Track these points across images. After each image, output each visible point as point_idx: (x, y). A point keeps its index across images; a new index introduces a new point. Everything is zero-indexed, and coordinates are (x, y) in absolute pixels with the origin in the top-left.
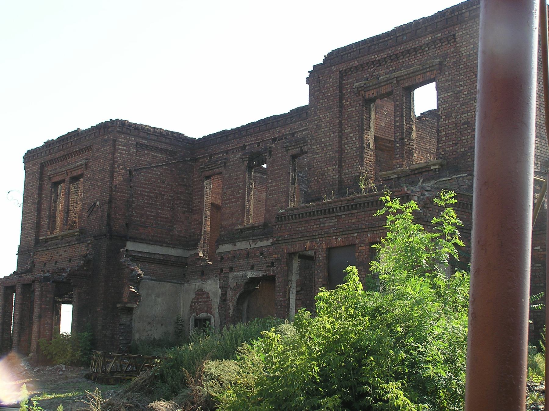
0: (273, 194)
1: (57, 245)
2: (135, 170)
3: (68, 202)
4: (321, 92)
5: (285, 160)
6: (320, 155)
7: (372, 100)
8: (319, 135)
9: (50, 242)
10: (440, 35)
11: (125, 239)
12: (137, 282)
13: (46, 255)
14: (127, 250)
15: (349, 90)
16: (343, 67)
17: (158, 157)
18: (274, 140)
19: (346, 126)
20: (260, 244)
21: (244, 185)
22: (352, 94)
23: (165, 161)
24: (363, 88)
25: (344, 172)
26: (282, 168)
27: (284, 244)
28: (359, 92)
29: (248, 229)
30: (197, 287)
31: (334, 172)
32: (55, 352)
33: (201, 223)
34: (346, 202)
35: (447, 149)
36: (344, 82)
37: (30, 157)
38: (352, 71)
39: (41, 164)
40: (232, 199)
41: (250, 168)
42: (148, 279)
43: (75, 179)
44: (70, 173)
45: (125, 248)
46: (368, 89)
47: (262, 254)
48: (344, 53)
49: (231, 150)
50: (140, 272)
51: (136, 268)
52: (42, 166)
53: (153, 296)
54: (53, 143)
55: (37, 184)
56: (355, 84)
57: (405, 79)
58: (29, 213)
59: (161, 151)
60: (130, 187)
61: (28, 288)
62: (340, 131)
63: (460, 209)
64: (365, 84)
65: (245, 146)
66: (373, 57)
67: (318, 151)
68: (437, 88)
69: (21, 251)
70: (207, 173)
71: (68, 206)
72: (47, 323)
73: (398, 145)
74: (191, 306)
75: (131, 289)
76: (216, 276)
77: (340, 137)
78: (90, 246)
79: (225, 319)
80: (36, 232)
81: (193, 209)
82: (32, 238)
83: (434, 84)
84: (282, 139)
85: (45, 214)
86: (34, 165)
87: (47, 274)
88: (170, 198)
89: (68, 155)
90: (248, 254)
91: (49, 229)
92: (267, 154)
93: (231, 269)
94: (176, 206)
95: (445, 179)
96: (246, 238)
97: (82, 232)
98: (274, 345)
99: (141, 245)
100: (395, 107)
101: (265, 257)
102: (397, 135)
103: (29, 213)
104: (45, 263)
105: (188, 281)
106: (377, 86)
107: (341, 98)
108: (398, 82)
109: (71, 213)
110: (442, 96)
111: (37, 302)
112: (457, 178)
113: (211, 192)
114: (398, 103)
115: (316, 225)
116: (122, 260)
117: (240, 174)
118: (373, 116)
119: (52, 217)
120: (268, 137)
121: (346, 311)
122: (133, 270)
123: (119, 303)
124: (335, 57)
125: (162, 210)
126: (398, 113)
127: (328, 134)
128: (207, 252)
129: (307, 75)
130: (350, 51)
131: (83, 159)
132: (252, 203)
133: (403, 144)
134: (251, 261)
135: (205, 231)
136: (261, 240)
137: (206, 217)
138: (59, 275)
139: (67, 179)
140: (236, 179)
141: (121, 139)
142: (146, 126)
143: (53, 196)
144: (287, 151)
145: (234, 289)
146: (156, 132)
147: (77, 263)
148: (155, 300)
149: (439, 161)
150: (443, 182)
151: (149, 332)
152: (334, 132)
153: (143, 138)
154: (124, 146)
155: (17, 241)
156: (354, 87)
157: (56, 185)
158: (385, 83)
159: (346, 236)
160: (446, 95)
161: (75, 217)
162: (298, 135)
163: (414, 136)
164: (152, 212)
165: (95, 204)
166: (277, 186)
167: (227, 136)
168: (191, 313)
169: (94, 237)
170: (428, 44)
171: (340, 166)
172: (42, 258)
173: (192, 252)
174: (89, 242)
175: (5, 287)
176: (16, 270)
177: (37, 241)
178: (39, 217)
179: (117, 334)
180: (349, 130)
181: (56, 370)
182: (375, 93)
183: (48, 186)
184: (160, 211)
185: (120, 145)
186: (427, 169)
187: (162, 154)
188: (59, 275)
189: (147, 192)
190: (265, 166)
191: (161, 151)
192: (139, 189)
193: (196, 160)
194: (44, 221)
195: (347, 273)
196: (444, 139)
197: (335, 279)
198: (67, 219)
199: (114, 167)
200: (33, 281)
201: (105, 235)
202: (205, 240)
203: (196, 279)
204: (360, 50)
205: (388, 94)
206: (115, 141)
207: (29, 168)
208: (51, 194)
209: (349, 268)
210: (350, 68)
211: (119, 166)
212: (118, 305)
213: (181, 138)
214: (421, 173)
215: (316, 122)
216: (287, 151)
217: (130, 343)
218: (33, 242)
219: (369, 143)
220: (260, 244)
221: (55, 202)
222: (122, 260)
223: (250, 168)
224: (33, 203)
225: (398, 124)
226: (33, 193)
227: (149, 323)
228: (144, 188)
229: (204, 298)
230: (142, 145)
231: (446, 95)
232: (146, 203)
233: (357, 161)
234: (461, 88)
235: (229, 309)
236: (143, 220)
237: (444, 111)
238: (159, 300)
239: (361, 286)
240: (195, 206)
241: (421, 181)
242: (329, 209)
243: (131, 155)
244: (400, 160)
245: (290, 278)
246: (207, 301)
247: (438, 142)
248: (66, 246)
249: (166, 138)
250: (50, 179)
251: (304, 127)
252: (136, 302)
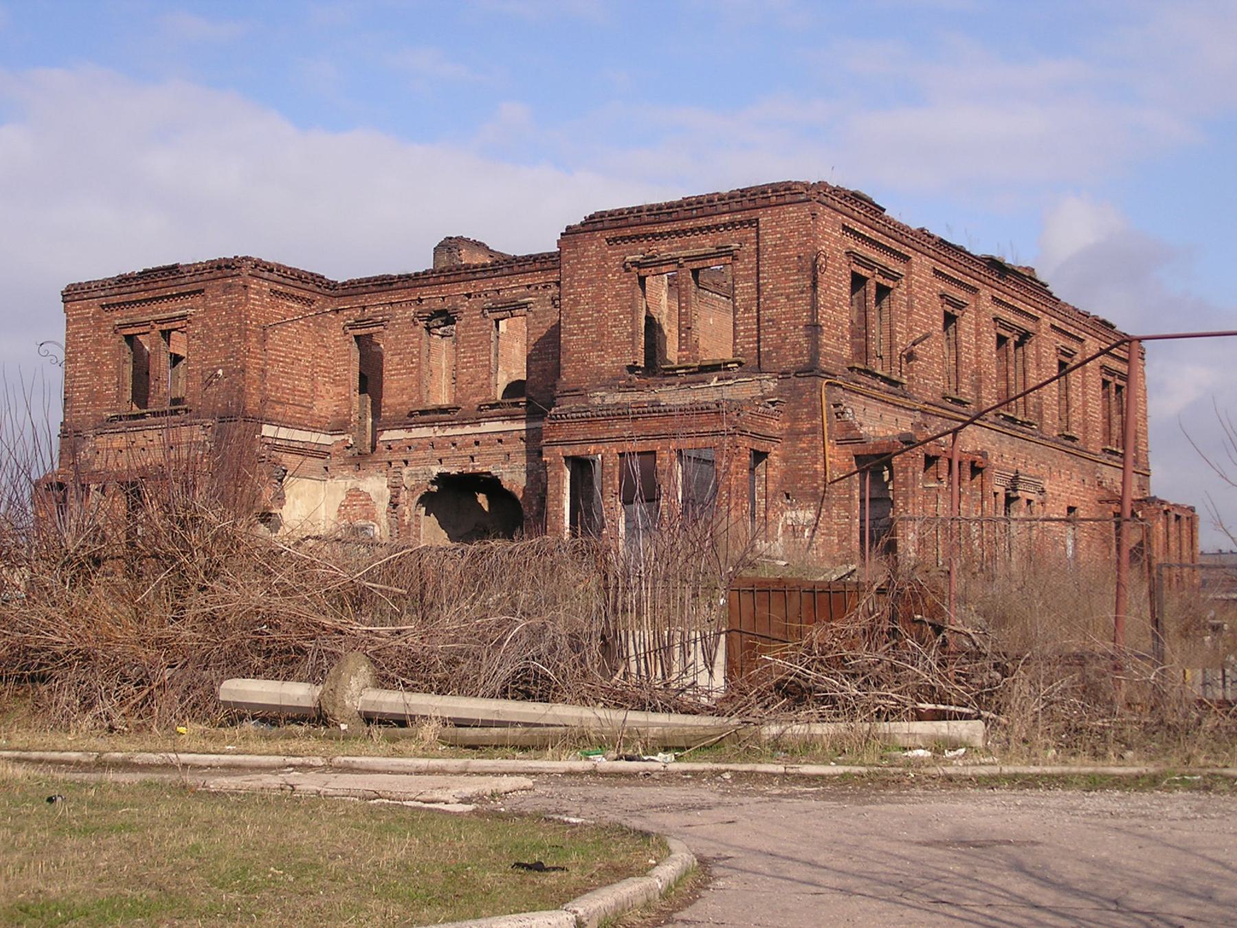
0: (467, 368)
11: (261, 420)
18: (469, 296)
47: (454, 445)
65: (421, 300)
125: (299, 380)
134: (438, 454)
154: (257, 294)
220: (450, 432)
238: (298, 502)
247: (735, 338)
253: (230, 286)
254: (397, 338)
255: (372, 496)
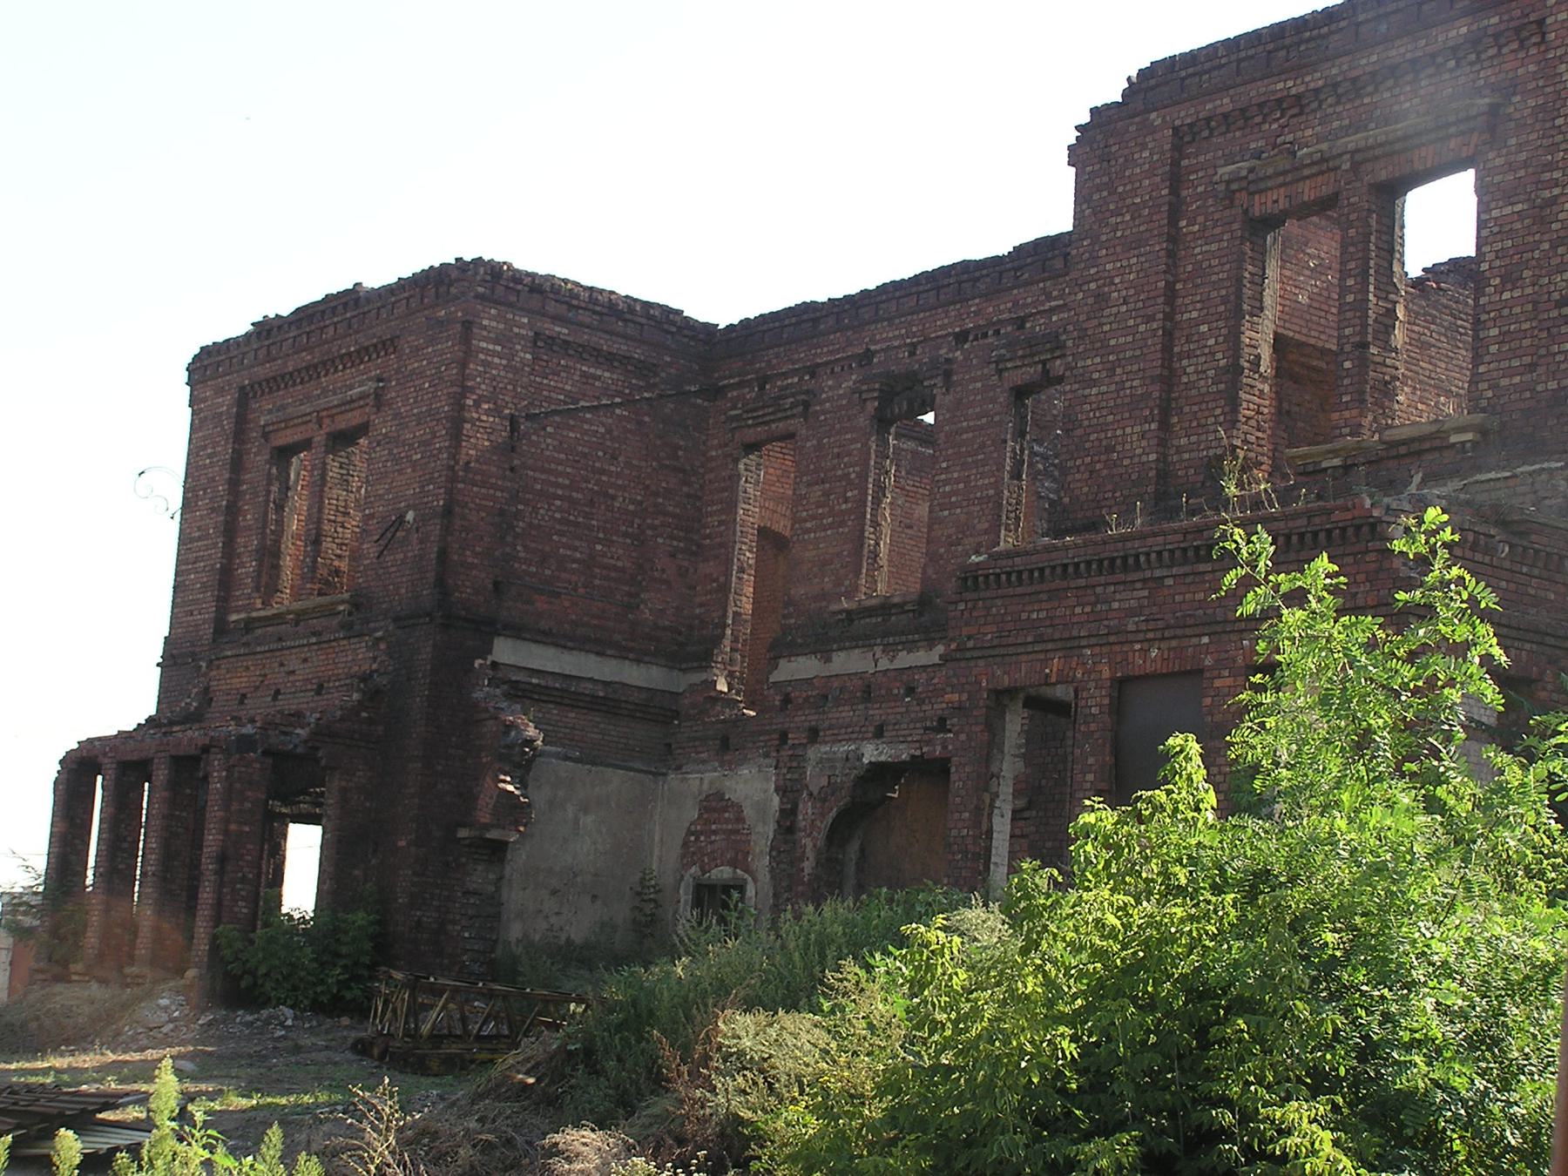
0: (953, 506)
1: (280, 639)
2: (528, 417)
3: (320, 510)
4: (1113, 192)
5: (993, 401)
6: (1104, 389)
7: (1272, 222)
8: (1101, 325)
9: (259, 631)
10: (1495, 20)
11: (487, 629)
12: (522, 764)
13: (247, 668)
14: (494, 665)
15: (1200, 189)
16: (1184, 115)
17: (599, 378)
18: (961, 337)
19: (1187, 301)
20: (905, 659)
21: (863, 476)
22: (1210, 201)
23: (620, 393)
24: (1244, 184)
25: (1175, 442)
26: (981, 428)
27: (981, 663)
28: (1230, 196)
29: (869, 612)
30: (705, 786)
31: (1144, 443)
32: (262, 970)
33: (724, 589)
34: (1180, 537)
35: (1504, 382)
36: (1185, 163)
37: (209, 367)
38: (1212, 130)
39: (242, 388)
40: (822, 516)
41: (882, 422)
42: (557, 756)
43: (343, 439)
44: (327, 421)
45: (490, 659)
46: (1262, 185)
47: (911, 691)
48: (1191, 70)
49: (827, 363)
50: (531, 731)
51: (521, 720)
52: (244, 398)
53: (571, 810)
54: (279, 327)
55: (226, 451)
56: (1220, 171)
57: (1376, 158)
58: (200, 539)
59: (609, 360)
60: (512, 469)
61: (188, 768)
62: (1168, 317)
63: (1536, 572)
64: (1251, 170)
66: (1280, 86)
67: (1096, 375)
68: (1480, 189)
69: (173, 656)
70: (750, 435)
71: (319, 521)
72: (243, 880)
73: (1347, 365)
74: (685, 844)
75: (501, 785)
76: (767, 755)
77: (1169, 335)
78: (382, 646)
79: (789, 889)
80: (218, 599)
81: (701, 541)
82: (205, 615)
83: (1467, 178)
84: (985, 335)
85: (248, 543)
86: (220, 392)
87: (249, 729)
88: (631, 507)
89: (324, 363)
90: (868, 691)
91: (257, 589)
92: (939, 381)
93: (814, 735)
94: (649, 532)
95: (1492, 475)
96: (863, 641)
97: (359, 603)
98: (940, 970)
99: (537, 649)
100: (1344, 247)
101: (921, 702)
102: (1347, 332)
103: (200, 539)
104: (244, 696)
105: (679, 768)
106: (1289, 178)
107: (1174, 214)
108: (1355, 166)
109: (328, 545)
110: (1495, 213)
111: (214, 812)
112: (1530, 474)
113: (759, 493)
114: (1352, 232)
115: (1083, 605)
116: (478, 695)
117: (853, 441)
118: (1272, 270)
119: (270, 555)
120: (942, 327)
121: (1166, 874)
122: (510, 727)
123: (464, 826)
124: (1160, 84)
126: (1352, 265)
127: (1131, 322)
128: (741, 679)
129: (1072, 137)
130: (1207, 66)
131: (369, 379)
132: (886, 530)
133: (1363, 363)
135: (735, 613)
136: (911, 647)
137: (742, 570)
138: (286, 734)
139: (319, 438)
140: (838, 456)
141: (489, 320)
142: (566, 281)
143: (274, 488)
144: (1000, 372)
145: (822, 798)
146: (596, 302)
147: (343, 698)
148: (576, 821)
149: (1478, 418)
150: (1486, 486)
151: (553, 920)
152: (1149, 319)
153: (556, 319)
155: (160, 626)
156: (1216, 178)
157: (284, 454)
158: (1314, 170)
159: (1174, 643)
160: (1508, 210)
161: (339, 556)
162: (1036, 326)
163: (1399, 337)
164: (575, 549)
165: (401, 517)
166: (966, 480)
167: (815, 321)
168: (687, 866)
169: (396, 619)
170: (1454, 49)
171: (1165, 425)
172: (232, 679)
173: (696, 678)
174: (379, 634)
175: (119, 763)
176: (153, 712)
177: (221, 628)
178: (229, 551)
179: (454, 922)
180: (1195, 314)
181: (267, 1022)
182: (1281, 201)
183: (258, 458)
184: (599, 547)
185: (485, 339)
186: (1437, 443)
187: (611, 369)
188: (286, 734)
189: (563, 487)
190: (929, 418)
191: (609, 360)
192: (537, 475)
193: (715, 392)
194: (242, 565)
195: (1168, 757)
196: (1494, 349)
197: (1131, 774)
198: (315, 561)
199: (462, 407)
200: (206, 749)
201: (429, 614)
202: (735, 640)
203: (704, 762)
204: (1239, 61)
205: (1325, 205)
206: (468, 325)
207: (204, 400)
208: (270, 484)
209: (1175, 741)
210: (1208, 120)
211: (477, 404)
212: (463, 833)
213: (673, 323)
214: (1419, 453)
215: (1093, 286)
216: (1000, 372)
217: (493, 950)
218: (208, 631)
219: (1258, 357)
220: (905, 659)
221: (280, 508)
222: (478, 695)
223: (882, 422)
224: (213, 510)
225: (1350, 298)
226: (213, 479)
227: (554, 892)
228: (550, 472)
229: (727, 821)
230: (551, 340)
231: (1508, 210)
232: (560, 521)
233: (1218, 411)
234: (1556, 191)
235: (802, 858)
236: (548, 572)
237: (1498, 263)
238: (588, 820)
239: (1211, 799)
240: (707, 537)
241: (1417, 479)
242: (1125, 558)
243: (516, 370)
244: (1355, 412)
245: (994, 769)
246: (737, 832)
247: (1476, 360)
248: (309, 645)
249: (625, 321)
250: (266, 436)
251: (1055, 299)
252: (516, 823)
253: (441, 323)
254: (819, 447)
255: (748, 812)
